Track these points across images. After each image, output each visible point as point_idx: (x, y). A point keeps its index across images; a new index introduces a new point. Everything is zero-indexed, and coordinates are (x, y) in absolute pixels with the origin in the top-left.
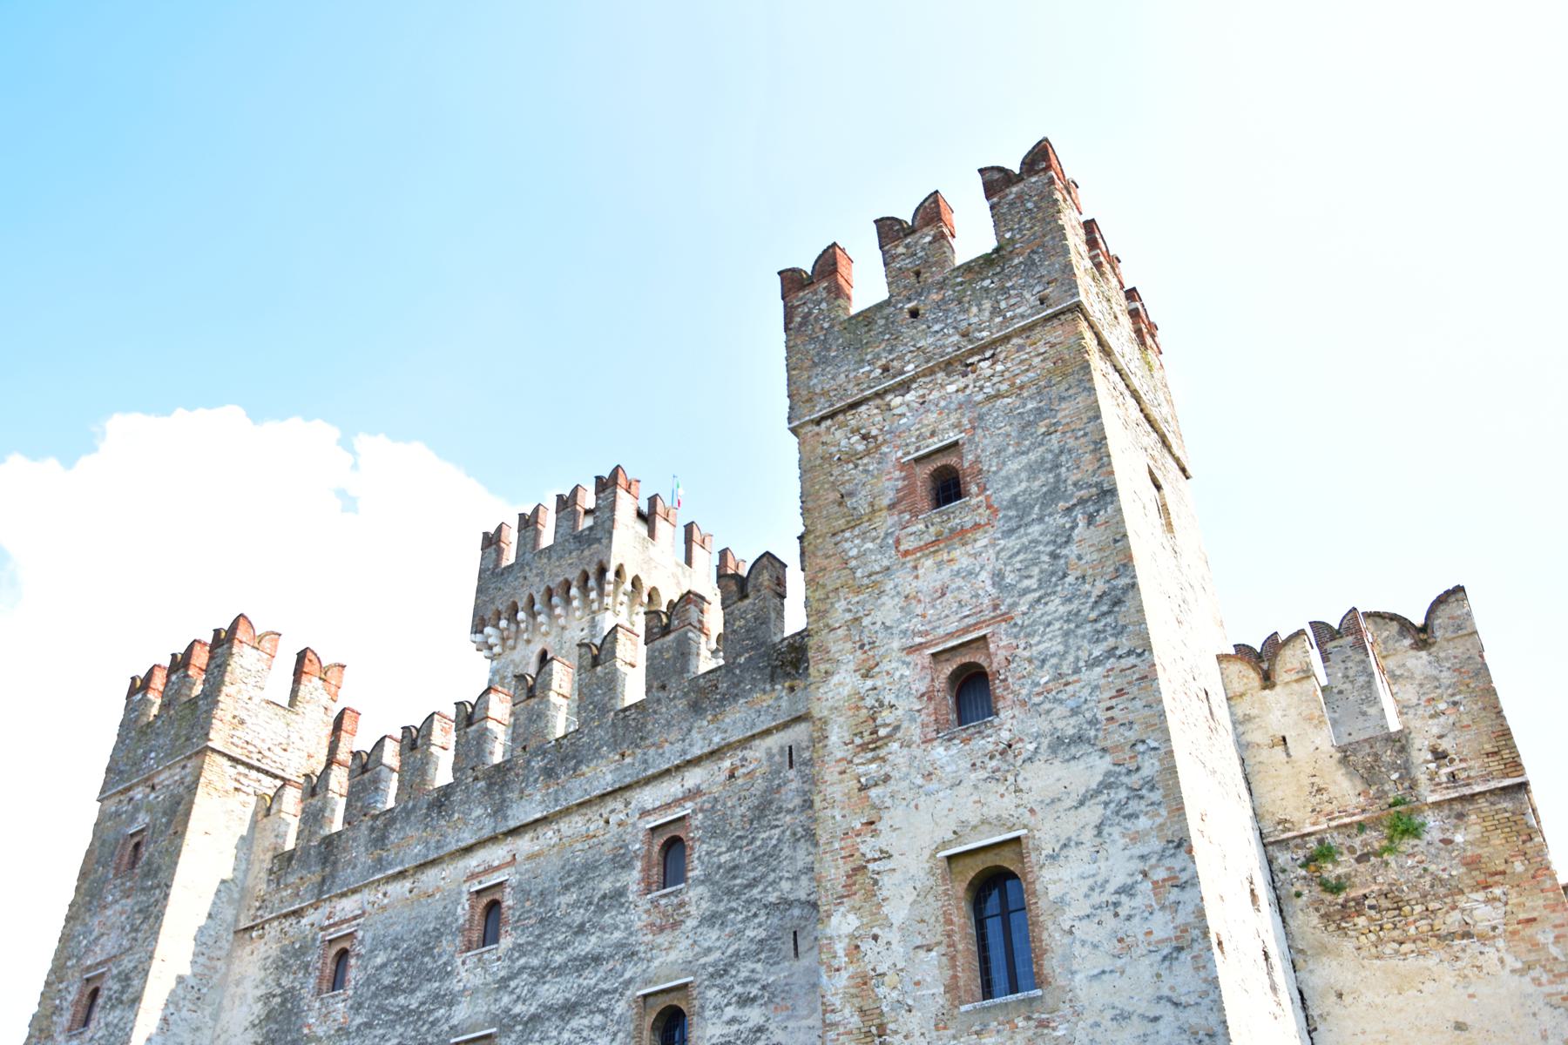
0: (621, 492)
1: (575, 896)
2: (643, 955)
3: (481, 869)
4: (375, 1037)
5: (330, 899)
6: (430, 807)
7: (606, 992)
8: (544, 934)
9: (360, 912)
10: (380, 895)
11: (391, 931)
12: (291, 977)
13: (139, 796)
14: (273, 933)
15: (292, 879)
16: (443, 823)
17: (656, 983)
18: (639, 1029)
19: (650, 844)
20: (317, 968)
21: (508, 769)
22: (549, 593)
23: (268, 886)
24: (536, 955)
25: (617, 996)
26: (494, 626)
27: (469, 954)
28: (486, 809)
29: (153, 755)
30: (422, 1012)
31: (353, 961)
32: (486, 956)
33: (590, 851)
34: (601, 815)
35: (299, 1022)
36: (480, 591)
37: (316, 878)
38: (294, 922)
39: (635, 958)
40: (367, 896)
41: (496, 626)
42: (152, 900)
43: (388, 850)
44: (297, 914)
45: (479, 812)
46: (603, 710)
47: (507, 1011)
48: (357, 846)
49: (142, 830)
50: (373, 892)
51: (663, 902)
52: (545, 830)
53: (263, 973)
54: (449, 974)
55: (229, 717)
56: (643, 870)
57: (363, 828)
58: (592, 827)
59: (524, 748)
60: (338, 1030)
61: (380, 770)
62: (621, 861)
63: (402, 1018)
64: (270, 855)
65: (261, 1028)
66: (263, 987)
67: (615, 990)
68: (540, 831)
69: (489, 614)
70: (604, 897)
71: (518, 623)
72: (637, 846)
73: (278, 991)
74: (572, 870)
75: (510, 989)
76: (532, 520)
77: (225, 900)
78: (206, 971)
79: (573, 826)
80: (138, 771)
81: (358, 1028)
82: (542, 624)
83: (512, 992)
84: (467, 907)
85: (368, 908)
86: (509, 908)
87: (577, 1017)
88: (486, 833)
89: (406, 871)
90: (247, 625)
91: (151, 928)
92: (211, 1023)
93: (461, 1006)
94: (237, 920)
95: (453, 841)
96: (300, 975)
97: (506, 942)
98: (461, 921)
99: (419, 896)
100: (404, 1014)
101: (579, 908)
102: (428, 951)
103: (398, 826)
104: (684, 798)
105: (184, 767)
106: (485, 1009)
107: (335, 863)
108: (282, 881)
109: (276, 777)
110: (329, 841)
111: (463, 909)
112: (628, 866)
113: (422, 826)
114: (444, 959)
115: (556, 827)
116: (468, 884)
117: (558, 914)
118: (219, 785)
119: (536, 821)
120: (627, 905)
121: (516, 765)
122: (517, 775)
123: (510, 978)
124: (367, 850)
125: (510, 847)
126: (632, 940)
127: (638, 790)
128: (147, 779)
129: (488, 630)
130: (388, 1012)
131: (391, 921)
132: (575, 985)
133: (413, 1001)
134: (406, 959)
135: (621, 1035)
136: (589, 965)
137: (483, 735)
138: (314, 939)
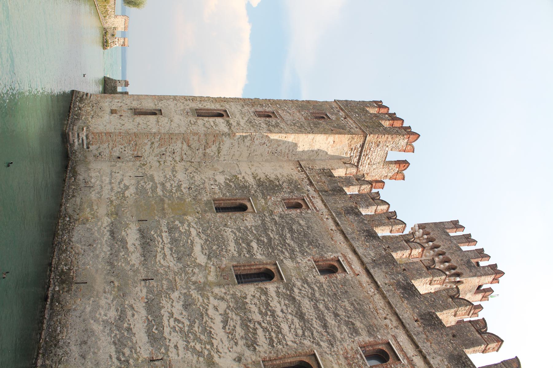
0: (493, 277)
1: (350, 309)
2: (332, 350)
3: (349, 260)
4: (272, 227)
5: (320, 196)
6: (368, 231)
7: (312, 334)
8: (330, 297)
9: (318, 209)
10: (326, 217)
11: (314, 225)
12: (287, 187)
13: (341, 114)
14: (301, 175)
15: (323, 179)
16: (363, 238)
17: (322, 360)
18: (300, 355)
19: (382, 344)
20: (292, 197)
21: (393, 264)
22: (443, 254)
23: (318, 170)
24: (320, 295)
25: (312, 340)
26: (423, 233)
27: (313, 262)
28: (374, 257)
29: (357, 115)
30: (285, 246)
31: (298, 211)
32: (314, 270)
33: (370, 313)
34: (387, 315)
35: (271, 194)
36: (435, 224)
37: (326, 188)
38: (307, 183)
39: (330, 346)
40: (325, 211)
41: (423, 234)
42: (306, 128)
43: (345, 216)
44: (311, 184)
45: (373, 254)
46: (433, 305)
47: (294, 285)
48: (343, 203)
49: (329, 118)
50: (327, 213)
51: (358, 356)
52: (373, 288)
53: (286, 175)
54: (303, 254)
55: (379, 140)
56: (370, 342)
57: (351, 203)
58: (381, 311)
59: (404, 270)
60: (271, 211)
61: (375, 206)
62: (371, 330)
63: (281, 237)
64: (330, 168)
65: (266, 179)
66: (281, 177)
67: (314, 339)
68: (372, 285)
69: (427, 230)
70: (353, 324)
71: (427, 242)
72: (380, 337)
73: (281, 183)
74: (360, 305)
75: (303, 285)
76: (470, 240)
77: (310, 154)
78: (283, 154)
79: (380, 303)
80: (350, 111)
81: (274, 219)
82: (429, 253)
83: (302, 286)
84: (332, 257)
85: (320, 213)
86: (336, 277)
87: (298, 321)
88: (365, 260)
89: (339, 226)
90: (415, 139)
91: (296, 130)
92: (264, 160)
93: (292, 263)
94: (302, 160)
95: (357, 245)
96: (288, 190)
97: (322, 278)
98: (326, 255)
99: (330, 234)
100: (283, 237)
101: (345, 312)
102: (310, 243)
103: (356, 218)
104: (408, 358)
105: (357, 128)
106: (293, 275)
107: (334, 195)
108: (321, 175)
109: (358, 163)
110: (341, 191)
111: (331, 255)
112: (370, 334)
113: (359, 229)
114: (309, 251)
115: (376, 293)
116: (341, 255)
117: (340, 302)
118: (353, 142)
119: (375, 283)
120: (353, 337)
121: (397, 267)
122: (393, 269)
123: (308, 284)
124: (343, 207)
125: (362, 272)
126: (338, 343)
127: (404, 332)
128: (348, 116)
129: (421, 231)
130: (282, 230)
131: (318, 224)
132: (312, 317)
133: (289, 240)
134: (305, 234)
135: (295, 345)
136: (322, 322)
137: (403, 248)
138: (303, 193)
